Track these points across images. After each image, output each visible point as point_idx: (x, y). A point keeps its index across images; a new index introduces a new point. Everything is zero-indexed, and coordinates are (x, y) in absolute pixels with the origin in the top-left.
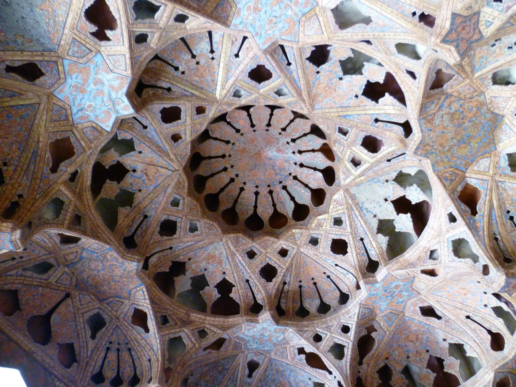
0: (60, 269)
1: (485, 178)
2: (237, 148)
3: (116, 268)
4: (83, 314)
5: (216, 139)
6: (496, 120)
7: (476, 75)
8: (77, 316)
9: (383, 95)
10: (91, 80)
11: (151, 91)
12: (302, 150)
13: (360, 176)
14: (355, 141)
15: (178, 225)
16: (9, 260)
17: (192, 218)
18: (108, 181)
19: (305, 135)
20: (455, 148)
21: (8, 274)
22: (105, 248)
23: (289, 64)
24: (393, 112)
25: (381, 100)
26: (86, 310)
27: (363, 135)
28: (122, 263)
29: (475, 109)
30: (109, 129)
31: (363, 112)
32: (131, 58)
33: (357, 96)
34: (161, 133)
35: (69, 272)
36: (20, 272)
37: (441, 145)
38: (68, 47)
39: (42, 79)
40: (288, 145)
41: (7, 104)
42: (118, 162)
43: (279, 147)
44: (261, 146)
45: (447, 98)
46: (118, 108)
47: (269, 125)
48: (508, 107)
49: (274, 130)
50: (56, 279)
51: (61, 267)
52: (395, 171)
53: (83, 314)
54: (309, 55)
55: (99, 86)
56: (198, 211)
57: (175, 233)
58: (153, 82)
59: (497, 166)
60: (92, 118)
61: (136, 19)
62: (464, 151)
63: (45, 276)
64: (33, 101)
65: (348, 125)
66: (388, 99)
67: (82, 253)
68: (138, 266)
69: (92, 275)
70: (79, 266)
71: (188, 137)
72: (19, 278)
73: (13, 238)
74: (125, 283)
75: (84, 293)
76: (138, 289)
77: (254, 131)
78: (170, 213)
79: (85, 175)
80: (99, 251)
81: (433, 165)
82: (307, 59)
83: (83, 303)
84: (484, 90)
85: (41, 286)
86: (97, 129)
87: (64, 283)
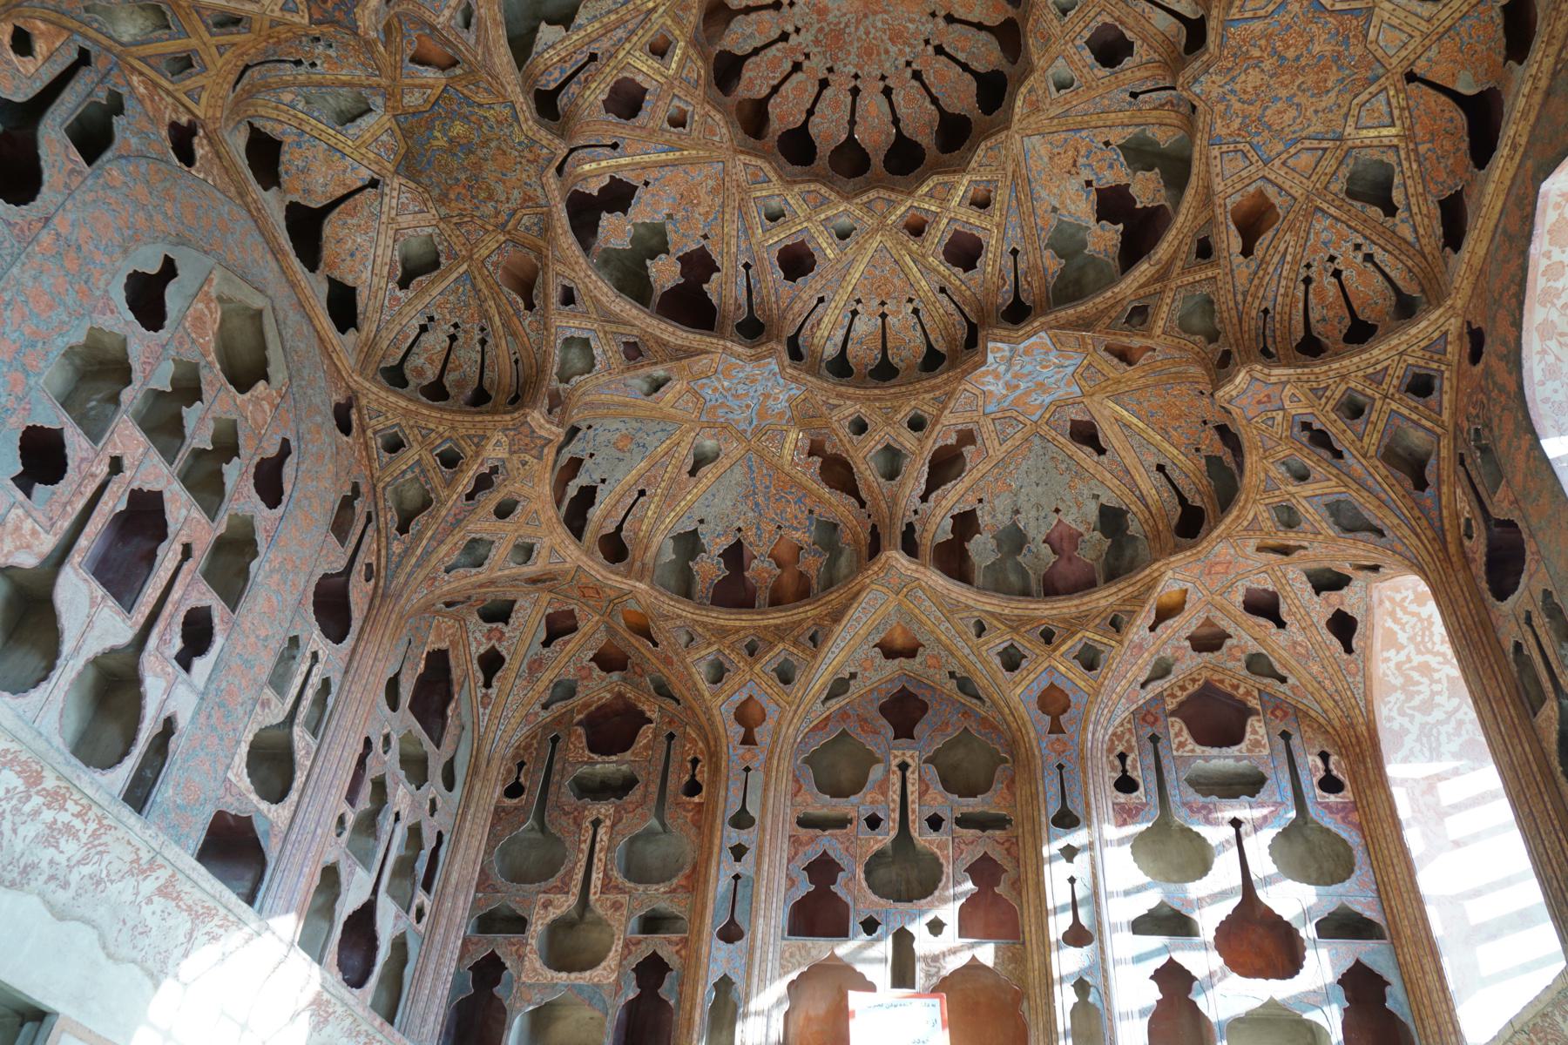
0: (1358, 142)
1: (408, 81)
2: (907, 50)
3: (1245, 92)
4: (1429, 21)
5: (934, 101)
6: (409, 166)
7: (465, 266)
8: (1441, 29)
9: (601, 190)
10: (1018, 392)
11: (966, 310)
12: (772, 12)
13: (654, 9)
14: (659, 98)
15: (1087, 34)
16: (1375, 265)
17: (1055, 22)
18: (1139, 206)
19: (756, 51)
20: (476, 140)
21: (1411, 237)
22: (1225, 148)
23: (747, 266)
24: (587, 167)
25: (607, 180)
26: (1413, 20)
27: (643, 117)
28: (1222, 99)
29: (452, 196)
30: (1043, 334)
31: (637, 158)
32: (945, 408)
33: (646, 184)
34: (998, 226)
35: (1351, 121)
36: (1401, 214)
37: (504, 153)
38: (1019, 435)
39: (1078, 418)
40: (800, 24)
41: (1141, 425)
42: (1098, 221)
43: (819, 21)
44: (857, 29)
45: (504, 225)
46: (1007, 354)
47: (824, 84)
48: (395, 194)
49: (817, 66)
50: (1385, 132)
51: (1350, 143)
52: (580, 27)
53: (1429, 21)
54: (715, 276)
55: (1015, 382)
56: (1037, 21)
57: (1105, 24)
58: (957, 317)
59: (389, 95)
60: (1055, 353)
61: (906, 456)
62: (458, 129)
63: (1389, 157)
64: (1112, 404)
65: (667, 136)
66: (593, 188)
67: (1279, 155)
68: (1196, 80)
69: (1313, 95)
70: (1316, 127)
71: (963, 185)
72: (1415, 209)
73: (1234, 393)
74: (1263, 42)
75: (1379, 53)
76: (1248, 15)
77: (856, 76)
78: (1085, 71)
79: (1136, 285)
80: (1240, 146)
81: (517, 119)
82: (718, 270)
83: (1404, 37)
84: (442, 225)
85: (1416, 150)
86: (1058, 344)
87: (1384, 108)
